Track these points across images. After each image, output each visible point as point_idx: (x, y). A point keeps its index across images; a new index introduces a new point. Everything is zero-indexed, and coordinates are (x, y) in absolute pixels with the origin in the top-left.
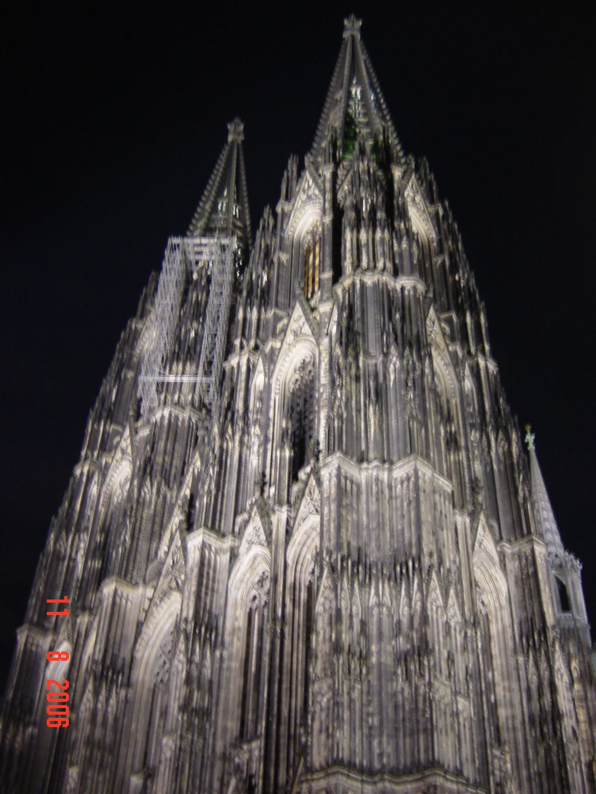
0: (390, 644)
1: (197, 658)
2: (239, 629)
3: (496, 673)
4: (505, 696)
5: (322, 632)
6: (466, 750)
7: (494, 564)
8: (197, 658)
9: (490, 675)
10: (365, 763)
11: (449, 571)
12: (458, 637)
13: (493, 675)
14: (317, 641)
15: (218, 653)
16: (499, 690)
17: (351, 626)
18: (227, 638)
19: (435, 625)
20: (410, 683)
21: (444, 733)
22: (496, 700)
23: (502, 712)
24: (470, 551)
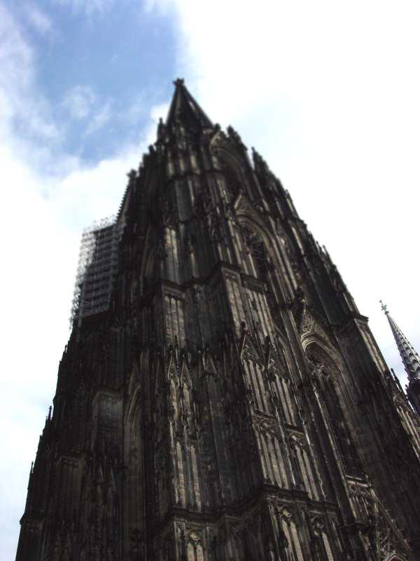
0: (220, 401)
1: (101, 480)
2: (135, 450)
3: (348, 423)
4: (359, 438)
5: (160, 409)
6: (306, 473)
7: (326, 344)
8: (101, 480)
9: (342, 424)
10: (208, 504)
11: (268, 339)
12: (284, 384)
13: (346, 426)
14: (157, 416)
15: (120, 474)
16: (354, 434)
17: (181, 396)
18: (127, 459)
19: (253, 373)
20: (237, 424)
21: (273, 456)
22: (351, 443)
23: (360, 452)
24: (296, 330)
